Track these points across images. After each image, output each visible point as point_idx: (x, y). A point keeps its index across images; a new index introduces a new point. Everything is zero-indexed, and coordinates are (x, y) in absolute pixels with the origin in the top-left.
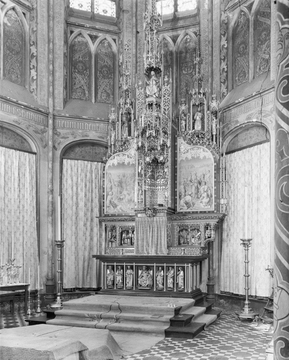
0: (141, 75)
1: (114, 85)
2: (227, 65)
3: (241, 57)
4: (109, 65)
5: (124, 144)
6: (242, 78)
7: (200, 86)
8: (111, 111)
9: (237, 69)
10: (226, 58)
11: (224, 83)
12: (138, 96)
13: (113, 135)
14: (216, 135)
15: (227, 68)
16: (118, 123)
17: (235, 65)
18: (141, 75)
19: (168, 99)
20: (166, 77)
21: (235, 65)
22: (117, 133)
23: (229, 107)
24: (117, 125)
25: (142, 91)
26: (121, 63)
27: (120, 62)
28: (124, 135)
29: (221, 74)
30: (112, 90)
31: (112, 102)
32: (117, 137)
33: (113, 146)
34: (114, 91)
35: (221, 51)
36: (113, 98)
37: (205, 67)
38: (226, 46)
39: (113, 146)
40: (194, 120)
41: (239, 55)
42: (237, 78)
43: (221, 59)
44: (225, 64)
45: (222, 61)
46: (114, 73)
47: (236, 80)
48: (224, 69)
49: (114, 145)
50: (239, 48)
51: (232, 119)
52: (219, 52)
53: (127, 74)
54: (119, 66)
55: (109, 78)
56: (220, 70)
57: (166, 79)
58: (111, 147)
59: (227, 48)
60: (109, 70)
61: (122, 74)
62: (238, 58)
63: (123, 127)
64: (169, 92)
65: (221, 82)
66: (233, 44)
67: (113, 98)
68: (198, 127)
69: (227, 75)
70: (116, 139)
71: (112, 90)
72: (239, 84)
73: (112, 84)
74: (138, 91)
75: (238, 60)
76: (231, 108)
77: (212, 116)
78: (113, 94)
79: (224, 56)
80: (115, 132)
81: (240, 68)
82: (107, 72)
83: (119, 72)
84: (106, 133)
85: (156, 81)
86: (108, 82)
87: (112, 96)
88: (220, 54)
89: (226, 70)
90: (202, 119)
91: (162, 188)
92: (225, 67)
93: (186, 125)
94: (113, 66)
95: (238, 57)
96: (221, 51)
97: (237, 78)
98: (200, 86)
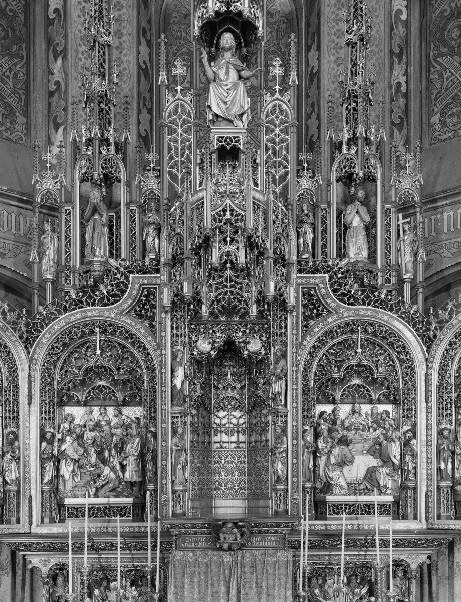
0: (125, 65)
1: (27, 82)
2: (406, 74)
3: (452, 56)
4: (10, 10)
5: (95, 281)
6: (456, 119)
7: (352, 121)
8: (43, 163)
9: (435, 92)
10: (405, 52)
11: (400, 127)
12: (170, 116)
13: (50, 253)
14: (413, 281)
15: (407, 82)
16: (67, 207)
17: (429, 80)
18: (125, 65)
19: (282, 141)
20: (277, 62)
21: (429, 80)
22: (63, 243)
23: (435, 201)
24: (64, 216)
25: (188, 99)
26: (56, 10)
27: (51, 8)
28: (97, 253)
29: (392, 100)
30: (23, 97)
31: (21, 139)
32: (63, 257)
33: (49, 288)
34: (27, 103)
35: (392, 29)
36: (27, 126)
37: (334, 72)
38: (404, 17)
39: (49, 288)
40: (344, 229)
41: (445, 50)
42: (436, 119)
43: (392, 53)
44: (403, 71)
45: (396, 60)
46: (28, 40)
47: (432, 126)
48: (399, 84)
49: (53, 282)
50: (444, 28)
51: (444, 237)
52: (388, 30)
53: (102, 40)
54: (50, 22)
55: (12, 56)
56: (390, 86)
57: (277, 70)
58: (42, 289)
59: (407, 24)
60: (13, 29)
61: (59, 49)
62: (440, 59)
63: (91, 224)
64: (287, 116)
65: (393, 124)
66: (423, 14)
67: (27, 126)
68: (357, 249)
69: (407, 106)
70: (63, 262)
71: (23, 97)
72: (446, 137)
73: (21, 76)
74: (171, 99)
75: (440, 64)
76: (440, 204)
77: (401, 221)
78: (26, 114)
79: (399, 46)
80: (59, 238)
81: (447, 89)
82: (6, 32)
83: (49, 41)
84: (12, 237)
85: (238, 71)
86: (10, 70)
87: (21, 119)
88: (392, 38)
89: (404, 89)
90: (370, 229)
91: (234, 439)
92: (403, 80)
93: (314, 240)
94: (26, 16)
95: (442, 55)
96: (392, 29)
97: (436, 119)
98: (352, 121)
